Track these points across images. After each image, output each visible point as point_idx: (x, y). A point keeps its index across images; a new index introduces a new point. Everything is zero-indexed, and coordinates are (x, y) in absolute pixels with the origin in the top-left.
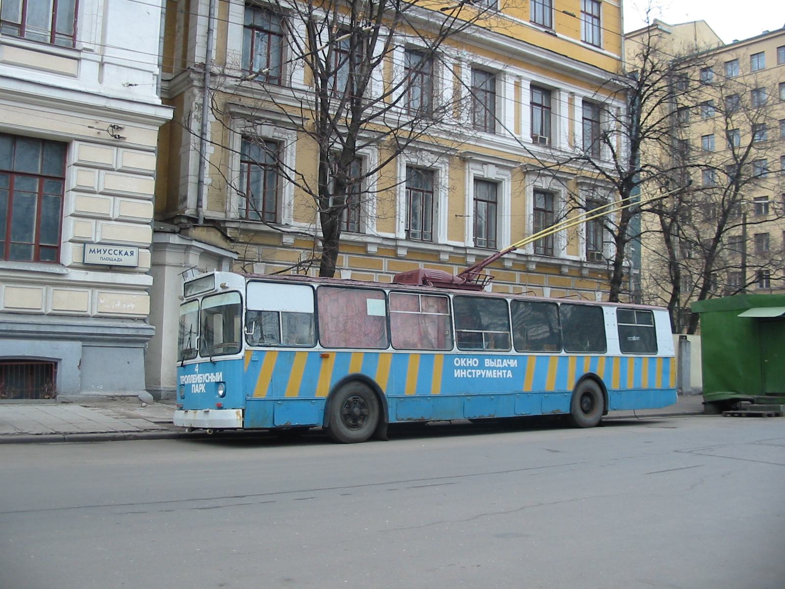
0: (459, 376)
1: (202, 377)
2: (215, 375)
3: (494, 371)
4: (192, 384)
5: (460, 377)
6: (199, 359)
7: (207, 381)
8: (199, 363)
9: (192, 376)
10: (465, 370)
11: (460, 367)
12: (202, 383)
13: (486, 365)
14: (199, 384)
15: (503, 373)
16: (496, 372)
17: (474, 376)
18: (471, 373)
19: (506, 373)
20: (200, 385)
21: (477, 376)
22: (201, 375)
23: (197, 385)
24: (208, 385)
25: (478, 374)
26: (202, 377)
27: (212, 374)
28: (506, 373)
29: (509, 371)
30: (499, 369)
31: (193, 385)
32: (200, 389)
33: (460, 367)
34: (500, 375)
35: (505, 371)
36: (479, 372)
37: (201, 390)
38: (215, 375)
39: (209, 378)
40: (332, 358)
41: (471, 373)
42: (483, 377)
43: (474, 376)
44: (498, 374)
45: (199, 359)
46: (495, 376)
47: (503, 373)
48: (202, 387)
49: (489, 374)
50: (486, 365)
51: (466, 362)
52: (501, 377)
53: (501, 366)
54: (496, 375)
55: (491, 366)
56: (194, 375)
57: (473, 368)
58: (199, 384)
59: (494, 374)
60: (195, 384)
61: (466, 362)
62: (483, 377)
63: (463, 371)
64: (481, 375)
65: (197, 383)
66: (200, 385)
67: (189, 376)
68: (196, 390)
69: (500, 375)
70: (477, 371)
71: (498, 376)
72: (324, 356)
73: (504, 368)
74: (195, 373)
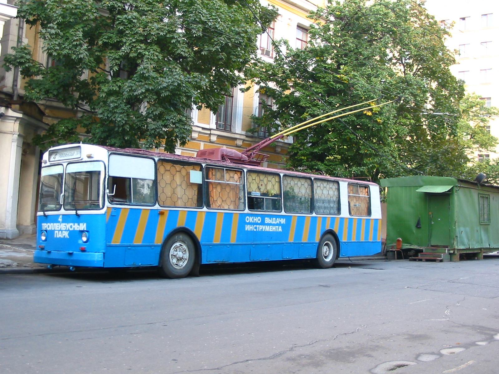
0: (248, 230)
1: (66, 226)
2: (79, 225)
3: (271, 226)
4: (55, 230)
5: (249, 231)
7: (71, 229)
8: (62, 215)
9: (55, 224)
10: (252, 226)
11: (250, 224)
12: (65, 231)
13: (266, 222)
15: (276, 228)
16: (272, 227)
17: (258, 230)
18: (256, 228)
19: (278, 228)
20: (63, 232)
21: (260, 230)
22: (65, 224)
24: (71, 233)
25: (260, 229)
26: (66, 226)
27: (76, 224)
28: (278, 228)
29: (280, 227)
30: (274, 225)
31: (56, 232)
32: (63, 235)
33: (250, 224)
34: (274, 230)
35: (277, 227)
36: (261, 227)
37: (64, 236)
38: (79, 225)
39: (73, 227)
40: (167, 214)
41: (256, 228)
42: (264, 230)
43: (258, 230)
44: (273, 229)
45: (63, 211)
46: (271, 231)
47: (276, 228)
48: (66, 234)
49: (267, 229)
50: (266, 222)
51: (253, 220)
52: (275, 231)
53: (275, 223)
54: (272, 229)
55: (269, 222)
56: (58, 224)
57: (257, 224)
58: (62, 231)
59: (271, 228)
60: (59, 231)
61: (253, 220)
62: (264, 230)
63: (251, 226)
64: (262, 229)
65: (60, 230)
66: (63, 232)
67: (52, 224)
68: (58, 235)
69: (274, 230)
70: (260, 226)
71: (273, 231)
72: (161, 213)
73: (277, 225)
74: (59, 222)
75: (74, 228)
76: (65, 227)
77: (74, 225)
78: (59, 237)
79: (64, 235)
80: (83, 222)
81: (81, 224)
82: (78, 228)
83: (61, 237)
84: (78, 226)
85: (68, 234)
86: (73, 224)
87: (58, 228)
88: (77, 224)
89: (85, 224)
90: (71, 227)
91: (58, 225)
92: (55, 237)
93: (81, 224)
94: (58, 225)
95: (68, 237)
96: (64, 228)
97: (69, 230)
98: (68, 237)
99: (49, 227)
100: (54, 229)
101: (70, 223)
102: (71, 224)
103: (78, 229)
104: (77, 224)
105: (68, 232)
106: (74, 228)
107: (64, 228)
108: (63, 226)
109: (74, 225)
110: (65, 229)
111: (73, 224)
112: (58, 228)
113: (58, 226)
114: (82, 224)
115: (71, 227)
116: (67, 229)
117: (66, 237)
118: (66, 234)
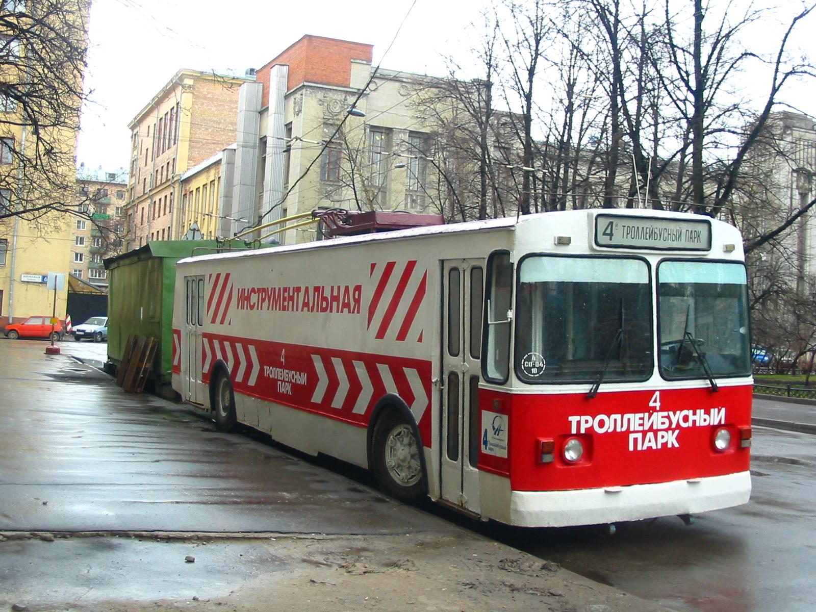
1: (668, 417)
2: (708, 412)
4: (628, 432)
6: (656, 382)
7: (684, 425)
9: (626, 416)
12: (666, 430)
14: (655, 432)
22: (665, 414)
23: (650, 435)
27: (701, 412)
31: (632, 437)
32: (660, 441)
37: (665, 445)
38: (708, 412)
39: (691, 418)
45: (656, 382)
48: (671, 439)
65: (651, 429)
66: (660, 434)
75: (694, 422)
76: (666, 421)
77: (694, 414)
78: (645, 448)
79: (664, 441)
80: (718, 406)
81: (712, 410)
82: (705, 420)
83: (654, 447)
84: (707, 417)
85: (677, 439)
86: (691, 412)
87: (642, 425)
88: (703, 411)
89: (723, 410)
90: (686, 419)
91: (642, 419)
92: (631, 448)
93: (712, 410)
94: (642, 419)
95: (677, 445)
96: (663, 423)
97: (678, 426)
98: (677, 445)
99: (602, 424)
100: (624, 429)
101: (681, 410)
102: (685, 412)
103: (706, 424)
104: (703, 411)
105: (677, 432)
106: (694, 422)
107: (663, 423)
108: (658, 419)
109: (694, 414)
110: (666, 426)
111: (691, 412)
112: (642, 425)
113: (641, 422)
114: (716, 410)
115: (686, 419)
116: (674, 426)
117: (670, 446)
118: (671, 439)
